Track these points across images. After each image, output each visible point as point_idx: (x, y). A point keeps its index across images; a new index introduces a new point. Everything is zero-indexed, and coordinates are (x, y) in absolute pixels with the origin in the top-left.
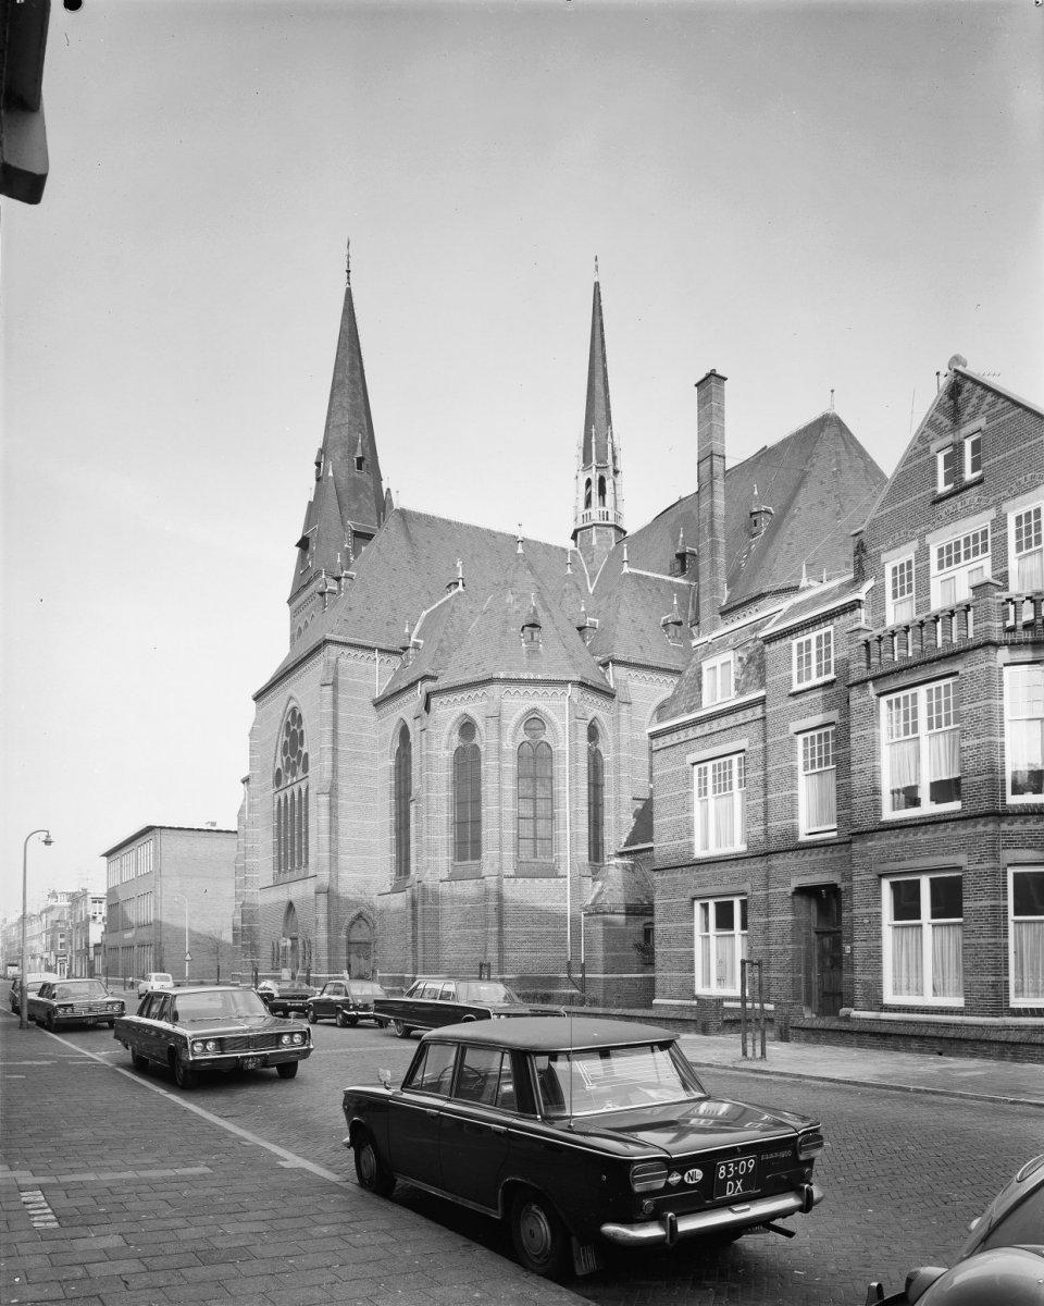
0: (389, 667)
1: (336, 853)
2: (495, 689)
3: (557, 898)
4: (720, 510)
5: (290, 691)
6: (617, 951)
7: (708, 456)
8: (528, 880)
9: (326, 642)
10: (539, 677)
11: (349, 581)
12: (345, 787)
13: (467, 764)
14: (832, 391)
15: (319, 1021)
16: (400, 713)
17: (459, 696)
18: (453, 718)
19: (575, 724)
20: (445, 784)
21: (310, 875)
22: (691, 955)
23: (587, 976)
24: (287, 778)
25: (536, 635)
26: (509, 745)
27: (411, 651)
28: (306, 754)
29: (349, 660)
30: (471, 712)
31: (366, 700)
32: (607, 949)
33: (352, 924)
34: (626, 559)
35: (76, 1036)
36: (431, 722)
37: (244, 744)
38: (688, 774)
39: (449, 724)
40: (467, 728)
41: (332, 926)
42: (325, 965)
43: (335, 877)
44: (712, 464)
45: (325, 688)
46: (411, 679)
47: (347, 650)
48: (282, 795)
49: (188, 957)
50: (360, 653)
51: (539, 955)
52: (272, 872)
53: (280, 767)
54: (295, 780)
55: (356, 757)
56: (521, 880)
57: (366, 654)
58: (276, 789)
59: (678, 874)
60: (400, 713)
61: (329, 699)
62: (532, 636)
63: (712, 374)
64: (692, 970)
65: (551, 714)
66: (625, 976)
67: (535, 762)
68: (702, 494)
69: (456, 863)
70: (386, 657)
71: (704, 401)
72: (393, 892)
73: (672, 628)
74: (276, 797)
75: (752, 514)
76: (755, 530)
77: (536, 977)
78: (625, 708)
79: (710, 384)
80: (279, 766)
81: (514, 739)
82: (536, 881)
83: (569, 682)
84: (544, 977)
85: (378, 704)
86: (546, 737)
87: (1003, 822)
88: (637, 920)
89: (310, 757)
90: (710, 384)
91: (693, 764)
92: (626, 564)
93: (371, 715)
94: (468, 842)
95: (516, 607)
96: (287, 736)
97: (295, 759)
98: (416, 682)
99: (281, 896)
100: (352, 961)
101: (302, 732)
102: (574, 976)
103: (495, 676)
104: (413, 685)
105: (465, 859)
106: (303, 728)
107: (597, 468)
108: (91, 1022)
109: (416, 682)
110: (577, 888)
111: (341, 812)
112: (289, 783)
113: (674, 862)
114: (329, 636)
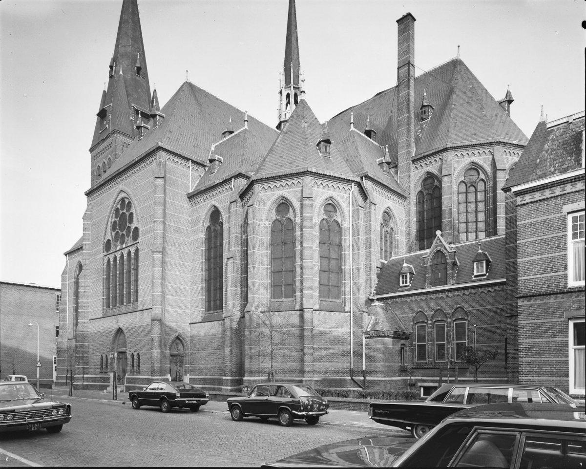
0: (197, 174)
1: (164, 294)
2: (308, 179)
3: (345, 326)
4: (412, 99)
5: (121, 186)
6: (389, 362)
7: (405, 64)
8: (327, 313)
9: (159, 148)
10: (336, 175)
11: (161, 119)
12: (170, 250)
13: (284, 235)
14: (459, 46)
15: (142, 407)
16: (213, 202)
17: (278, 184)
18: (273, 199)
19: (358, 210)
20: (265, 245)
21: (139, 309)
22: (566, 363)
23: (368, 378)
24: (116, 246)
25: (328, 148)
26: (317, 220)
27: (217, 163)
28: (136, 229)
29: (173, 164)
30: (287, 195)
31: (184, 193)
32: (386, 361)
33: (173, 342)
34: (352, 121)
35: (25, 445)
36: (256, 201)
37: (80, 223)
38: (565, 221)
39: (269, 203)
40: (283, 205)
41: (162, 343)
42: (158, 371)
43: (163, 311)
44: (409, 68)
45: (158, 180)
46: (226, 176)
47: (172, 157)
48: (111, 257)
49: (39, 364)
50: (180, 161)
51: (334, 364)
52: (102, 308)
53: (110, 238)
54: (124, 246)
55: (178, 230)
56: (323, 313)
57: (184, 162)
58: (105, 253)
59: (552, 300)
60: (213, 202)
61: (160, 188)
62: (326, 149)
63: (409, 15)
64: (567, 375)
65: (341, 202)
66: (394, 378)
67: (331, 233)
68: (400, 87)
69: (273, 300)
70: (196, 167)
71: (401, 32)
72: (203, 322)
73: (386, 166)
74: (106, 259)
75: (423, 106)
76: (424, 116)
77: (333, 380)
78: (373, 207)
79: (406, 22)
80: (109, 237)
81: (318, 216)
82: (332, 313)
83: (353, 181)
84: (336, 380)
85: (191, 197)
86: (337, 217)
87: (525, 300)
88: (398, 342)
89: (140, 230)
90: (406, 22)
91: (569, 213)
92: (352, 125)
93: (186, 204)
94: (285, 282)
95: (310, 130)
96: (116, 217)
97: (124, 232)
98: (230, 179)
99: (111, 324)
100: (172, 368)
101: (132, 214)
102: (356, 378)
103: (309, 170)
104: (227, 181)
105: (210, 310)
106: (133, 210)
107: (294, 87)
108: (34, 429)
109: (230, 179)
110: (358, 320)
111: (167, 267)
112: (118, 249)
113: (546, 289)
114: (161, 144)
